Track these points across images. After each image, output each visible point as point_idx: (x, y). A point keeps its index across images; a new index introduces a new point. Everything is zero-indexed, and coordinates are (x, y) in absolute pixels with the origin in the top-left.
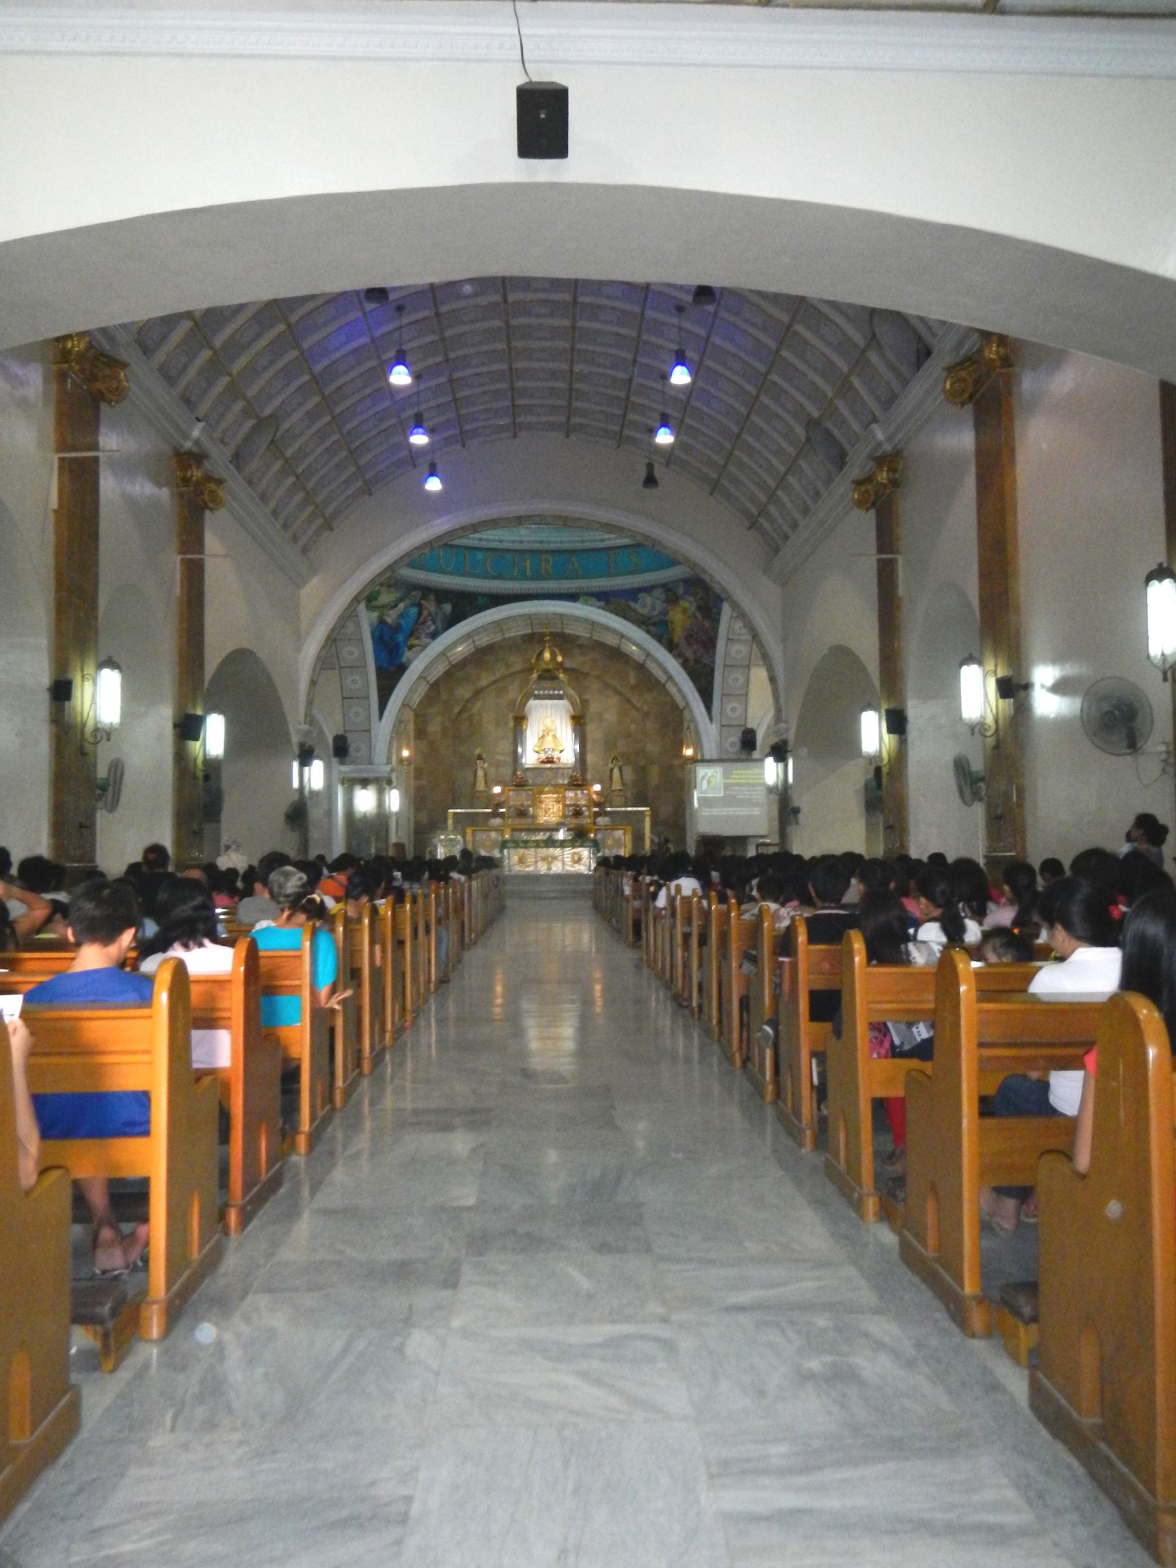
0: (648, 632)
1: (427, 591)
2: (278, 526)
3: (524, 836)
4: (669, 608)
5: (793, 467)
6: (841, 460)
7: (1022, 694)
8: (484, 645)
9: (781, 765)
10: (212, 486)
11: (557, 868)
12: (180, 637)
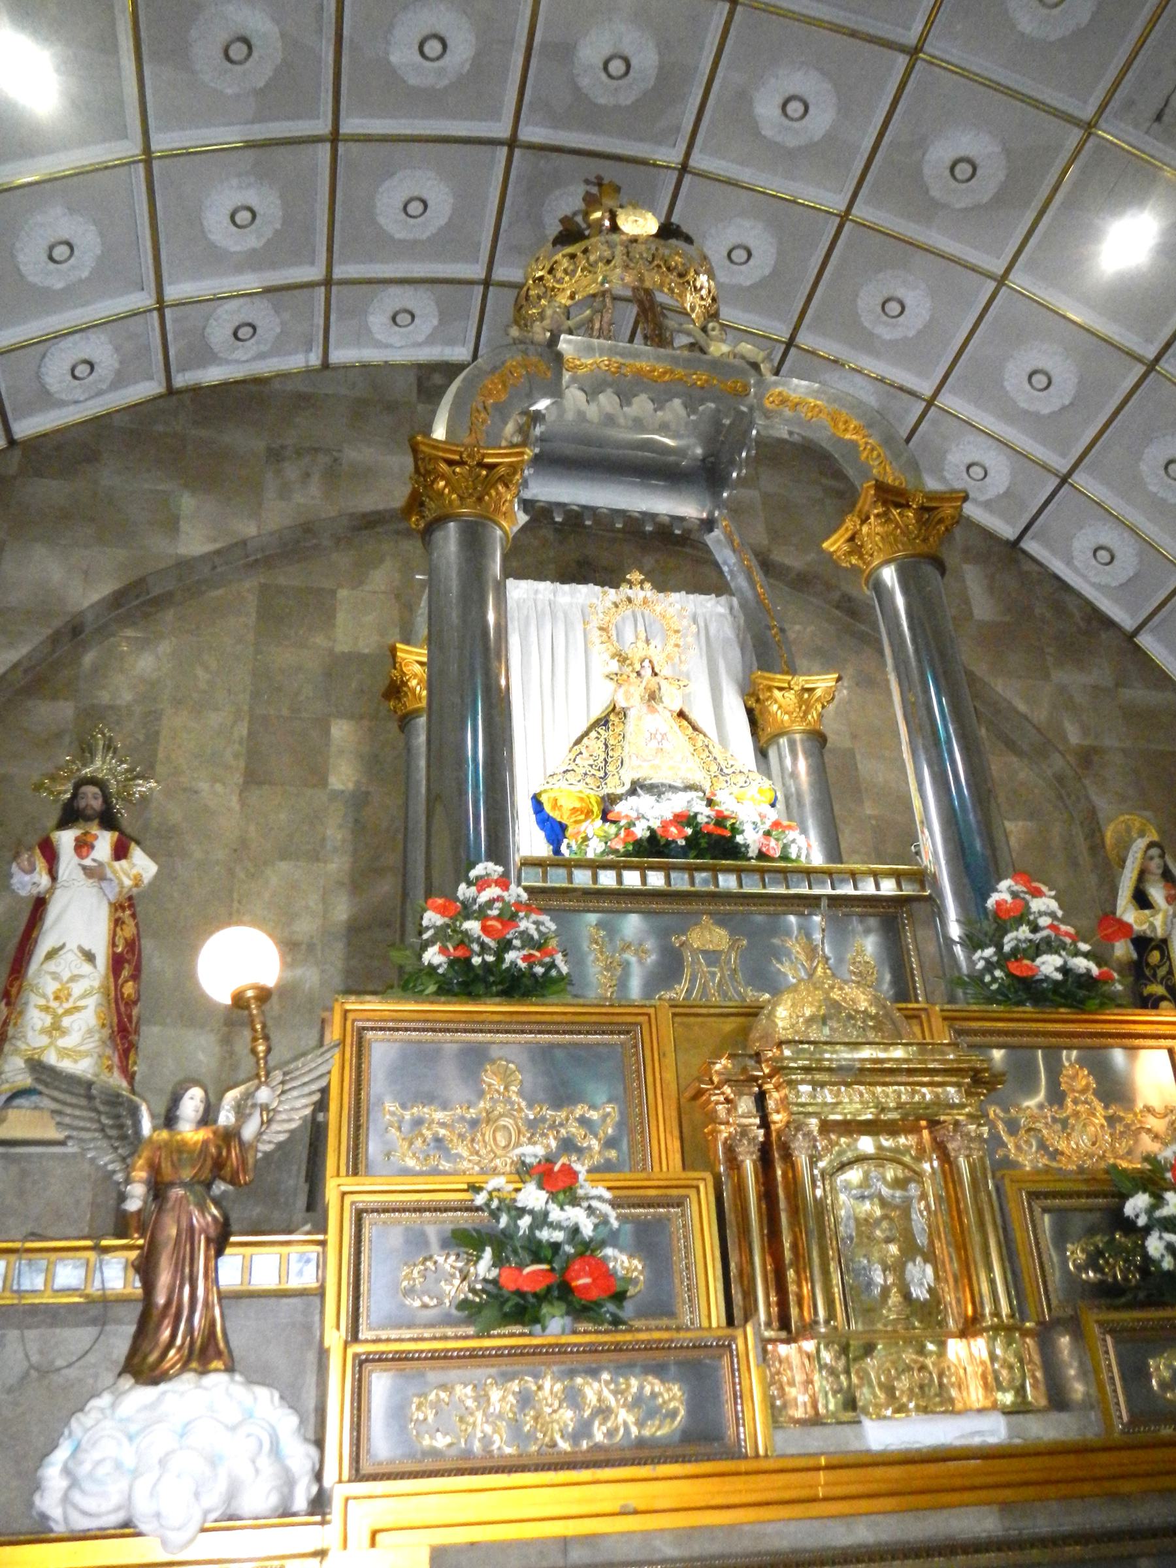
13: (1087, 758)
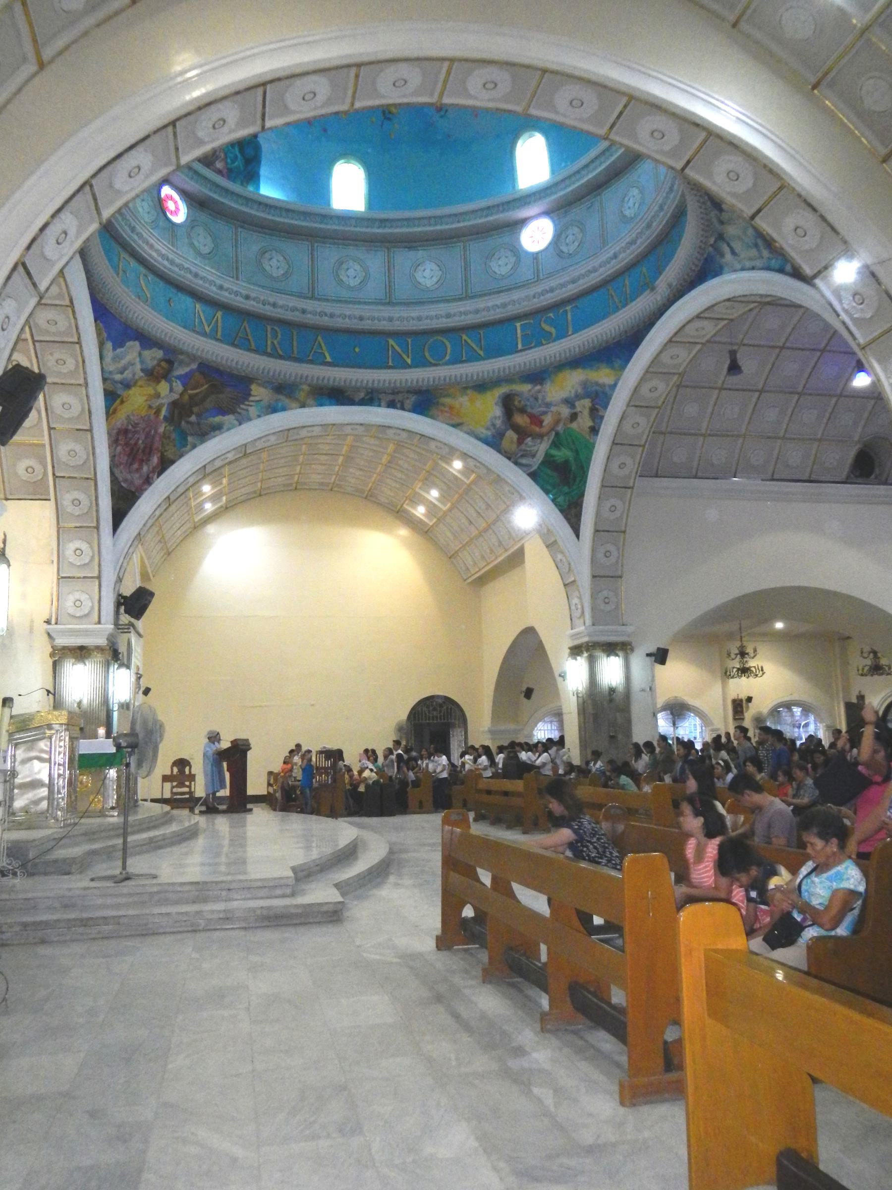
4: (139, 383)
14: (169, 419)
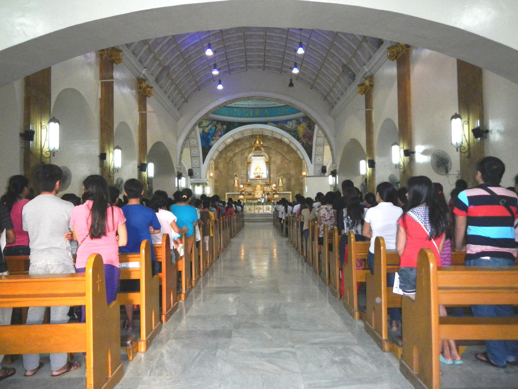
0: (291, 134)
1: (218, 121)
2: (170, 101)
3: (251, 201)
5: (338, 80)
6: (353, 77)
7: (412, 155)
8: (237, 139)
9: (334, 178)
10: (149, 89)
11: (261, 212)
12: (139, 138)
13: (290, 161)
14: (310, 129)
